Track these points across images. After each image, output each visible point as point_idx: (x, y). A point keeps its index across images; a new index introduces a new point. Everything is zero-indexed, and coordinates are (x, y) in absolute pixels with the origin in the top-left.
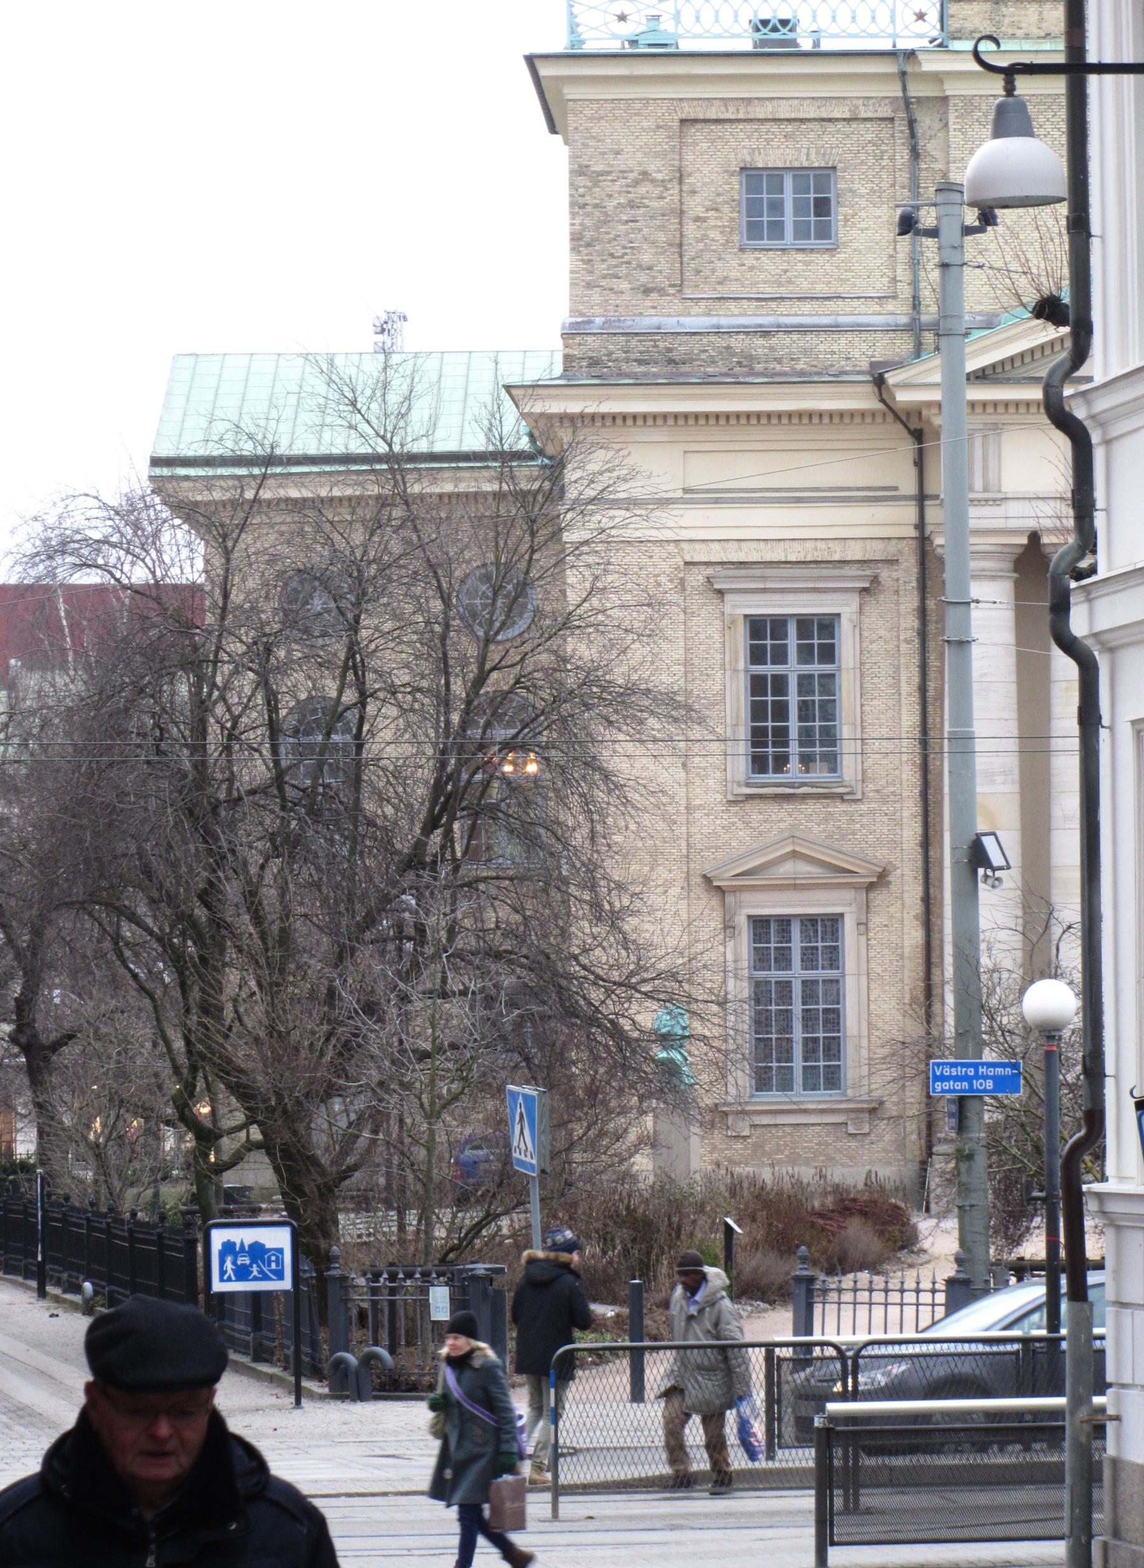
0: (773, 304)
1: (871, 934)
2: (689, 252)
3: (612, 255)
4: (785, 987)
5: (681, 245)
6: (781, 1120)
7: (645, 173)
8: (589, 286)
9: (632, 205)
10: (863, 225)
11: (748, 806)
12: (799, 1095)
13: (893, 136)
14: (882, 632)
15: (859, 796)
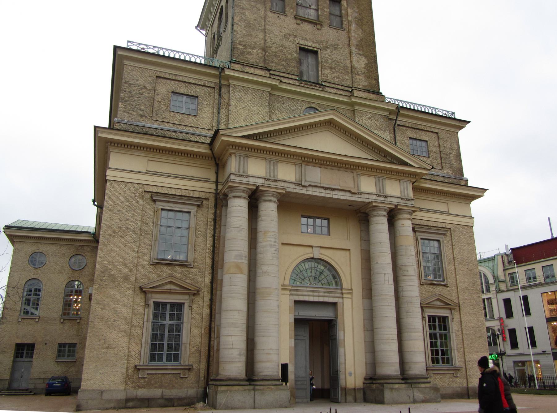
0: (178, 126)
1: (193, 310)
2: (155, 109)
3: (132, 105)
4: (163, 326)
5: (153, 107)
6: (158, 372)
7: (145, 87)
8: (124, 112)
9: (140, 93)
10: (205, 112)
11: (157, 267)
12: (164, 363)
13: (214, 92)
14: (202, 219)
15: (192, 266)
